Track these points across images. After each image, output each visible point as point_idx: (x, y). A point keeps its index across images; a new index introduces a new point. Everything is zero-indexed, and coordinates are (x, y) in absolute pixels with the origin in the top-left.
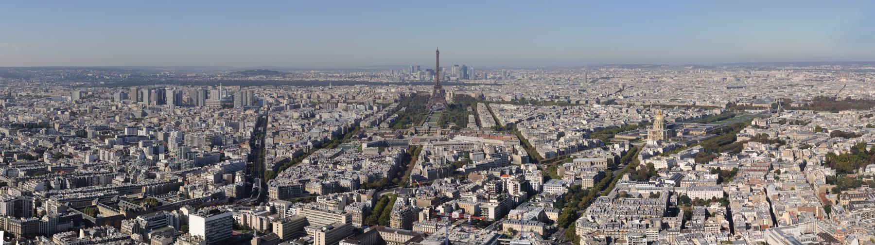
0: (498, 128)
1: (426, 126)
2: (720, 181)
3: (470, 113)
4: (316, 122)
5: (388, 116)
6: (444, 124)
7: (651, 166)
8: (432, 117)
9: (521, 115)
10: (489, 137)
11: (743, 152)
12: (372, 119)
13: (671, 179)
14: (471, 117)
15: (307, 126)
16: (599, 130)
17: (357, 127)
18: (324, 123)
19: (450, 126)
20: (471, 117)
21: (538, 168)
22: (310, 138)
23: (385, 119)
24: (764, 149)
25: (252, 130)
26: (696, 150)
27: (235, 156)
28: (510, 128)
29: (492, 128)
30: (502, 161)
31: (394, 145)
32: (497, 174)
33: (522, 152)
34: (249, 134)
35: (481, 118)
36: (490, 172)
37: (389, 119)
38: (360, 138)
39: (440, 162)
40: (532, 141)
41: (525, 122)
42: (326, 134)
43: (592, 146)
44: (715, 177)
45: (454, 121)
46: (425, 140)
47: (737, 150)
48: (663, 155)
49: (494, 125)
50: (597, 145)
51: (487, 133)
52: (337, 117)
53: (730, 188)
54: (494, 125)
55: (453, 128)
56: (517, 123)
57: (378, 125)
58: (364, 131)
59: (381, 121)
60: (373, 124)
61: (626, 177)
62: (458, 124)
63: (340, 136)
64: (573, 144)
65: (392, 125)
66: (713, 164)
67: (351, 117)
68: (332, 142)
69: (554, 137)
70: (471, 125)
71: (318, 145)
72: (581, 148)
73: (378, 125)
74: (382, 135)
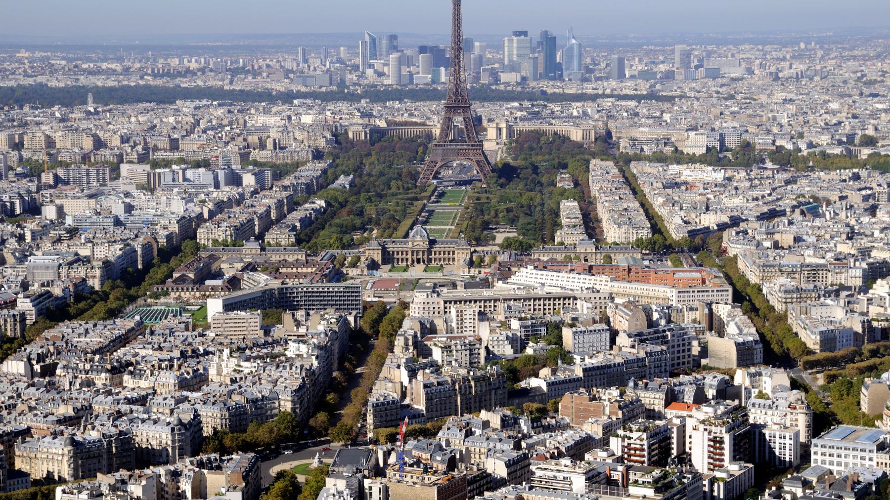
0: (659, 245)
1: (418, 239)
3: (564, 194)
4: (45, 229)
5: (294, 204)
6: (478, 231)
8: (439, 208)
9: (737, 201)
12: (239, 215)
14: (569, 208)
15: (12, 243)
17: (187, 245)
18: (73, 232)
19: (500, 238)
20: (569, 208)
21: (795, 385)
22: (25, 286)
23: (281, 216)
28: (701, 245)
29: (639, 244)
30: (670, 356)
31: (314, 302)
32: (653, 399)
33: (739, 328)
36: (630, 393)
37: (295, 217)
38: (200, 281)
39: (465, 357)
41: (754, 227)
42: (81, 271)
45: (512, 222)
46: (415, 284)
49: (645, 234)
51: (621, 260)
52: (118, 210)
54: (645, 234)
55: (507, 245)
56: (722, 227)
57: (260, 237)
58: (213, 258)
59: (268, 224)
60: (243, 233)
62: (524, 232)
63: (130, 278)
65: (306, 236)
67: (165, 211)
68: (104, 296)
69: (854, 277)
70: (569, 233)
71: (54, 311)
73: (260, 237)
74: (274, 270)
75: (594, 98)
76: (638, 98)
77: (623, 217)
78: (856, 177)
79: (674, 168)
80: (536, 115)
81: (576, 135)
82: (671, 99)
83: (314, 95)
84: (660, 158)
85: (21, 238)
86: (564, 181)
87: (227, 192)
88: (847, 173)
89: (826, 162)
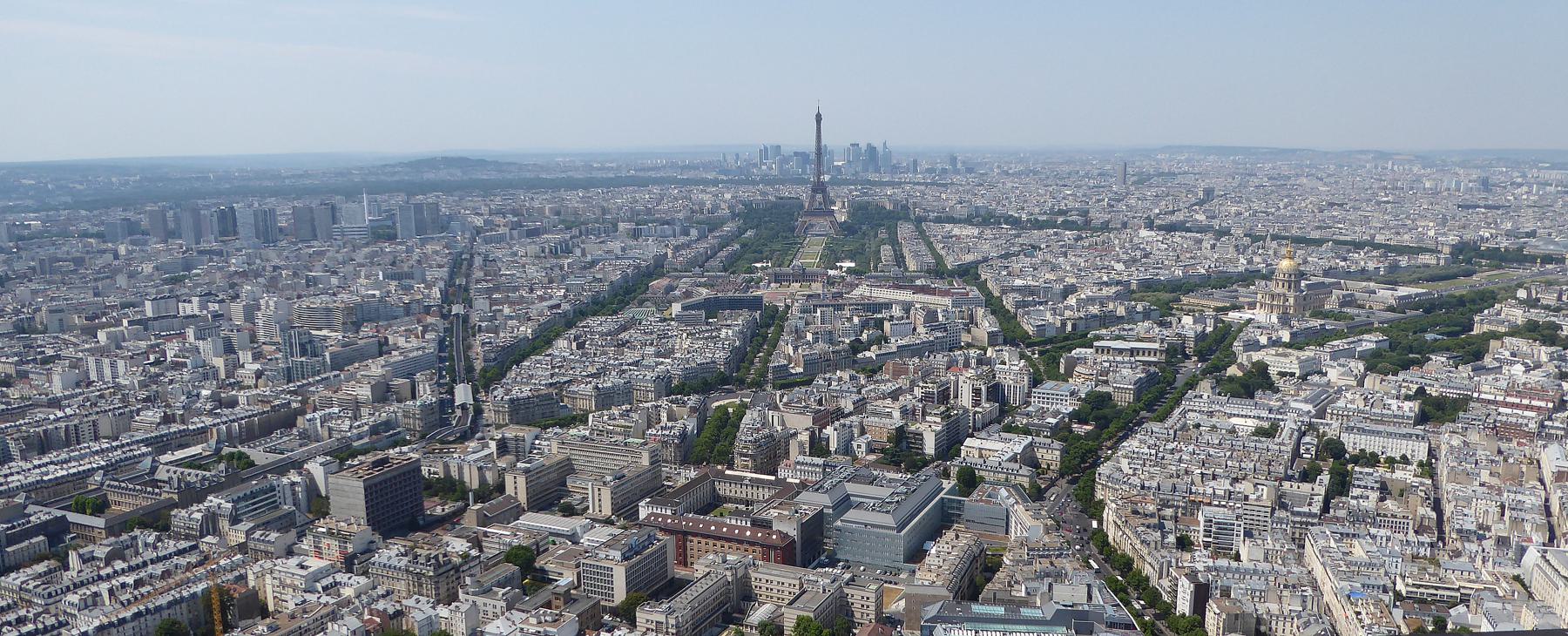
0: (938, 271)
2: (1422, 418)
3: (883, 242)
7: (1262, 368)
10: (924, 290)
11: (1488, 360)
13: (1306, 401)
14: (886, 251)
16: (1148, 286)
20: (886, 251)
21: (1022, 356)
24: (1544, 358)
25: (442, 284)
26: (1369, 343)
27: (408, 342)
28: (968, 273)
29: (929, 272)
34: (436, 292)
35: (906, 252)
40: (1009, 302)
43: (1131, 317)
44: (1410, 408)
47: (1473, 353)
48: (1287, 345)
50: (1146, 315)
53: (1448, 438)
55: (849, 270)
56: (976, 264)
61: (1205, 388)
64: (1094, 310)
66: (1410, 379)
67: (649, 249)
72: (1107, 320)
75: (900, 184)
76: (927, 184)
77: (916, 255)
78: (1056, 234)
79: (948, 227)
80: (865, 194)
81: (889, 207)
82: (945, 185)
83: (731, 181)
84: (938, 220)
85: (562, 268)
86: (883, 234)
87: (683, 240)
88: (1051, 231)
89: (1039, 225)
